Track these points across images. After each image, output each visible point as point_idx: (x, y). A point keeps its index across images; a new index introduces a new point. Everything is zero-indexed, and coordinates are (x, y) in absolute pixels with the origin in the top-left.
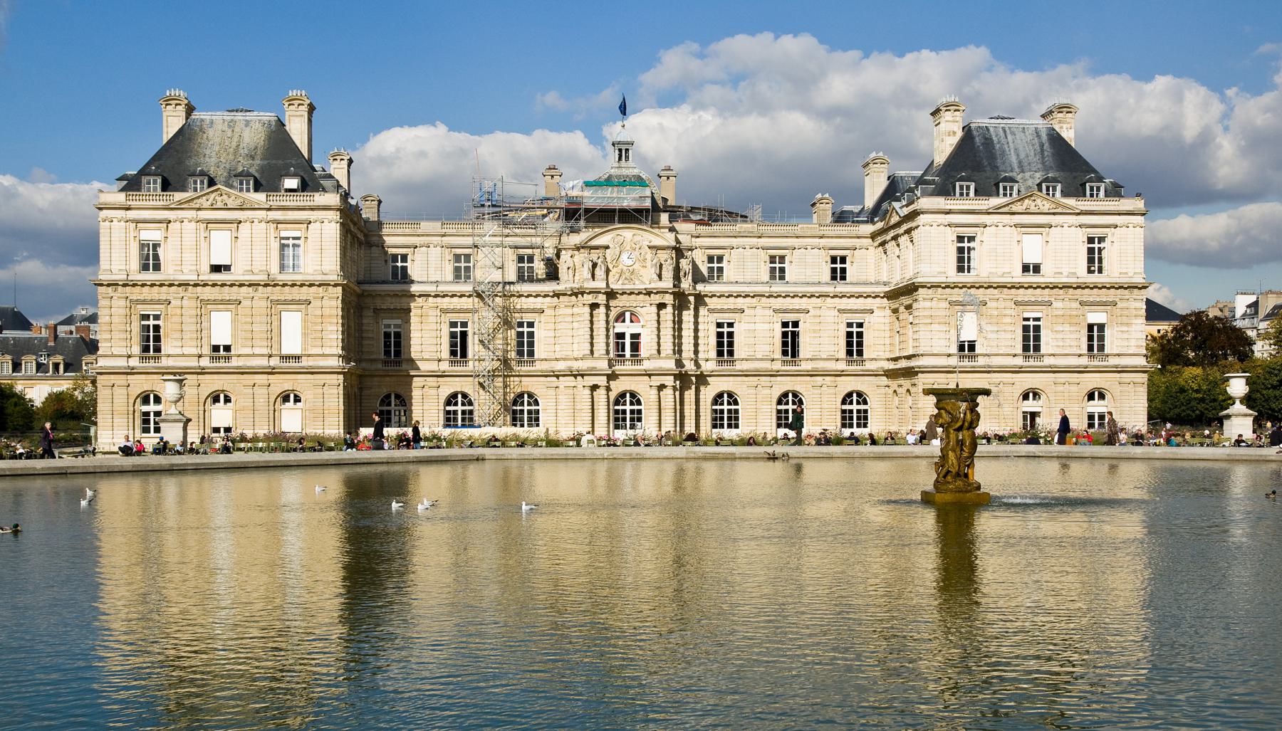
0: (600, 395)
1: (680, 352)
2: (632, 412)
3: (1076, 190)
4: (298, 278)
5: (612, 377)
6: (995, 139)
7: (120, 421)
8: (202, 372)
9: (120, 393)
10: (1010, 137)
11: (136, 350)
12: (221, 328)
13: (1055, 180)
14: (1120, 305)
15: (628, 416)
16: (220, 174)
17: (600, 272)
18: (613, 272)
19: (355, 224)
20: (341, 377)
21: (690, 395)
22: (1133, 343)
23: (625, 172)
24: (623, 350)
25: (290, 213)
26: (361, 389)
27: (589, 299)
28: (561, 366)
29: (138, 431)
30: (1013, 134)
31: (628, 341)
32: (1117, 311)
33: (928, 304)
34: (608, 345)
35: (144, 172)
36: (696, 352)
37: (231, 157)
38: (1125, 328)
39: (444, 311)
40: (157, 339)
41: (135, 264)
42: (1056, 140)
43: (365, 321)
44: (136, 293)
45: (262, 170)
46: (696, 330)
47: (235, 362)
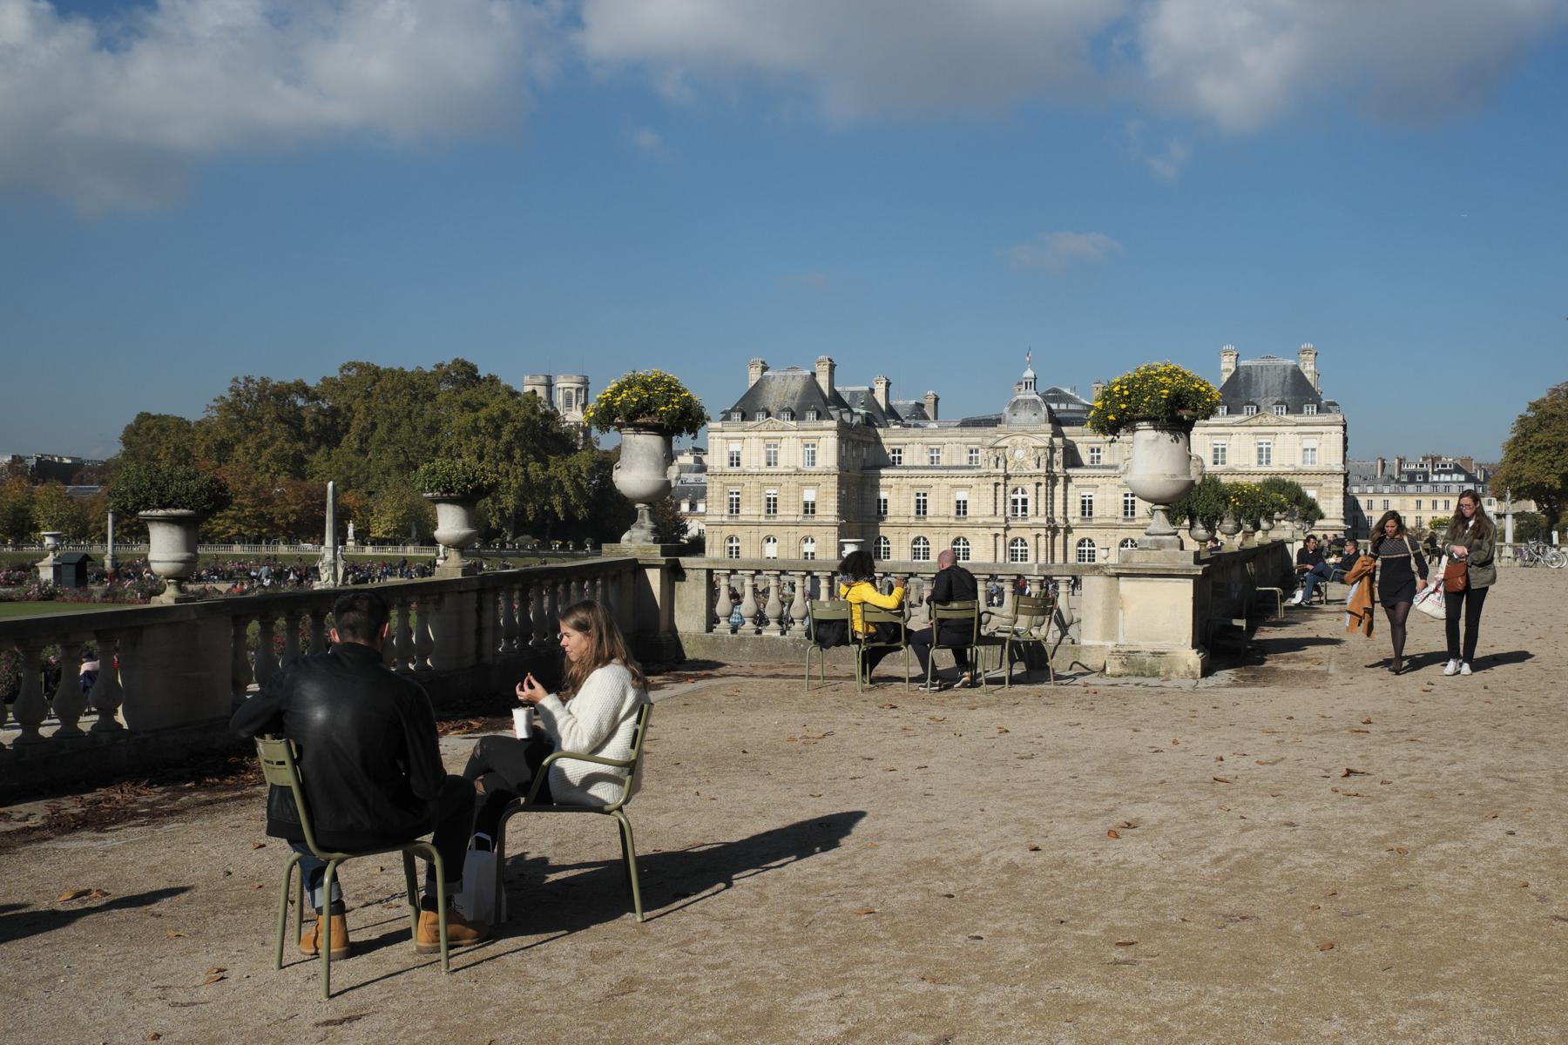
0: (1000, 540)
3: (1296, 409)
4: (813, 470)
5: (1007, 528)
8: (760, 524)
9: (717, 536)
11: (726, 512)
13: (1282, 403)
16: (772, 408)
17: (1001, 464)
18: (1010, 463)
21: (1059, 539)
27: (994, 480)
28: (980, 521)
31: (1020, 506)
35: (733, 410)
36: (1065, 513)
39: (913, 487)
41: (726, 462)
42: (1297, 375)
44: (726, 480)
45: (798, 407)
46: (1065, 499)
47: (779, 519)
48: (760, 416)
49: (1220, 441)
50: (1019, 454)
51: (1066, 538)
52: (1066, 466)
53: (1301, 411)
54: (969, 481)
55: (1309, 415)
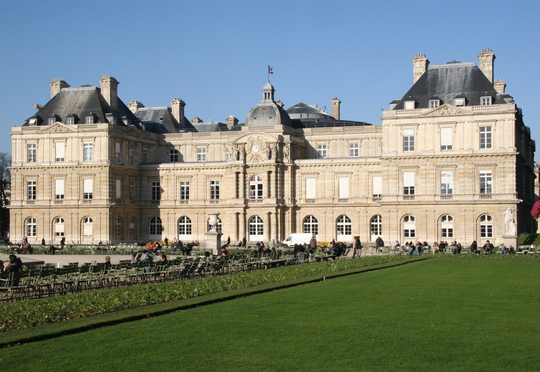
1: (283, 195)
2: (258, 226)
6: (440, 75)
7: (19, 230)
8: (50, 207)
9: (19, 217)
10: (449, 73)
12: (60, 188)
14: (499, 166)
15: (256, 228)
16: (62, 115)
17: (241, 157)
19: (137, 137)
20: (108, 209)
21: (288, 215)
22: (507, 187)
23: (267, 105)
24: (254, 195)
25: (88, 133)
26: (141, 215)
29: (26, 235)
30: (451, 71)
31: (256, 190)
32: (497, 169)
33: (386, 168)
34: (245, 192)
37: (71, 108)
38: (503, 179)
39: (178, 177)
40: (34, 193)
41: (25, 160)
43: (143, 182)
44: (25, 173)
47: (64, 203)
48: (52, 122)
49: (408, 133)
50: (255, 149)
51: (294, 215)
52: (293, 158)
53: (477, 103)
54: (220, 172)
55: (486, 107)
